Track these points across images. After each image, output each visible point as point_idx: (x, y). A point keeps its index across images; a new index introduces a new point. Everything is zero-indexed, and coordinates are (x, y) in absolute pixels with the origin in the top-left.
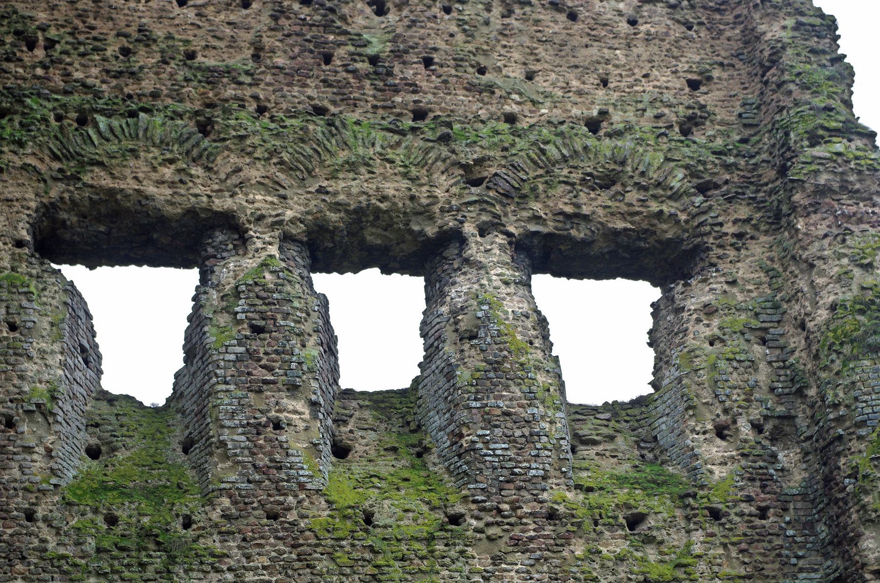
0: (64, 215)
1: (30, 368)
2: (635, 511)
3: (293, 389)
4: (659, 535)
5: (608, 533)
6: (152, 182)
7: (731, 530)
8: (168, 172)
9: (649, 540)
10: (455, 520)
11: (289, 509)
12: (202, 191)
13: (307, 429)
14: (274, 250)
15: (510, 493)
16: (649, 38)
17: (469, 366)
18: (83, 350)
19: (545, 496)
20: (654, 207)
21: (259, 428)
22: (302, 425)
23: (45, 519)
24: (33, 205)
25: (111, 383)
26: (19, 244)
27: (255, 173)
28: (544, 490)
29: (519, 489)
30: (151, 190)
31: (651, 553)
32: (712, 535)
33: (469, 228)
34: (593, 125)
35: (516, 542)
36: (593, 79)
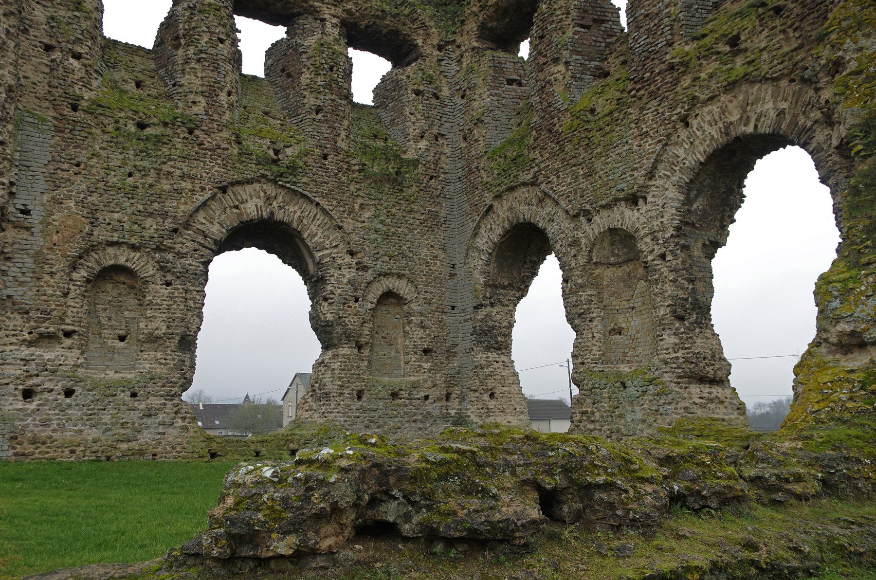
0: (490, 25)
1: (475, 104)
2: (730, 36)
3: (556, 61)
4: (748, 44)
5: (705, 63)
7: (788, 17)
11: (555, 125)
13: (564, 78)
15: (649, 64)
18: (510, 82)
19: (668, 57)
22: (561, 77)
23: (483, 169)
24: (475, 29)
26: (473, 49)
28: (666, 53)
29: (653, 60)
32: (773, 28)
35: (652, 95)
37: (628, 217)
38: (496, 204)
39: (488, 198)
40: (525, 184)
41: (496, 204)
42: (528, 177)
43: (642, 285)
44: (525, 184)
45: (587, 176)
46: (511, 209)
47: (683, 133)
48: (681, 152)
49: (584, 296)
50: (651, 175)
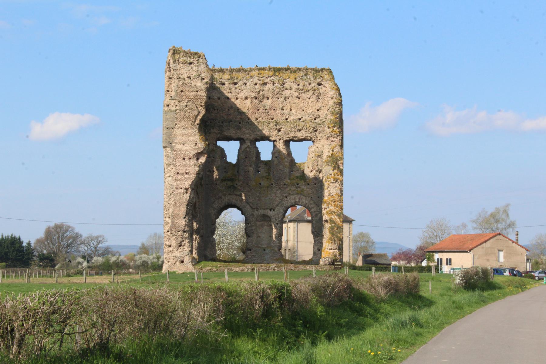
3: (251, 166)
6: (232, 132)
8: (234, 132)
9: (299, 187)
10: (272, 184)
12: (239, 135)
14: (249, 144)
16: (312, 102)
17: (276, 162)
20: (307, 135)
21: (246, 172)
25: (229, 160)
27: (247, 132)
30: (232, 135)
31: (299, 189)
33: (278, 140)
34: (300, 119)
35: (280, 188)
36: (301, 110)
37: (270, 213)
38: (223, 196)
39: (220, 194)
40: (236, 195)
41: (223, 196)
42: (239, 193)
43: (265, 227)
44: (236, 195)
45: (259, 200)
46: (228, 200)
47: (285, 199)
48: (285, 203)
49: (254, 228)
50: (277, 206)
